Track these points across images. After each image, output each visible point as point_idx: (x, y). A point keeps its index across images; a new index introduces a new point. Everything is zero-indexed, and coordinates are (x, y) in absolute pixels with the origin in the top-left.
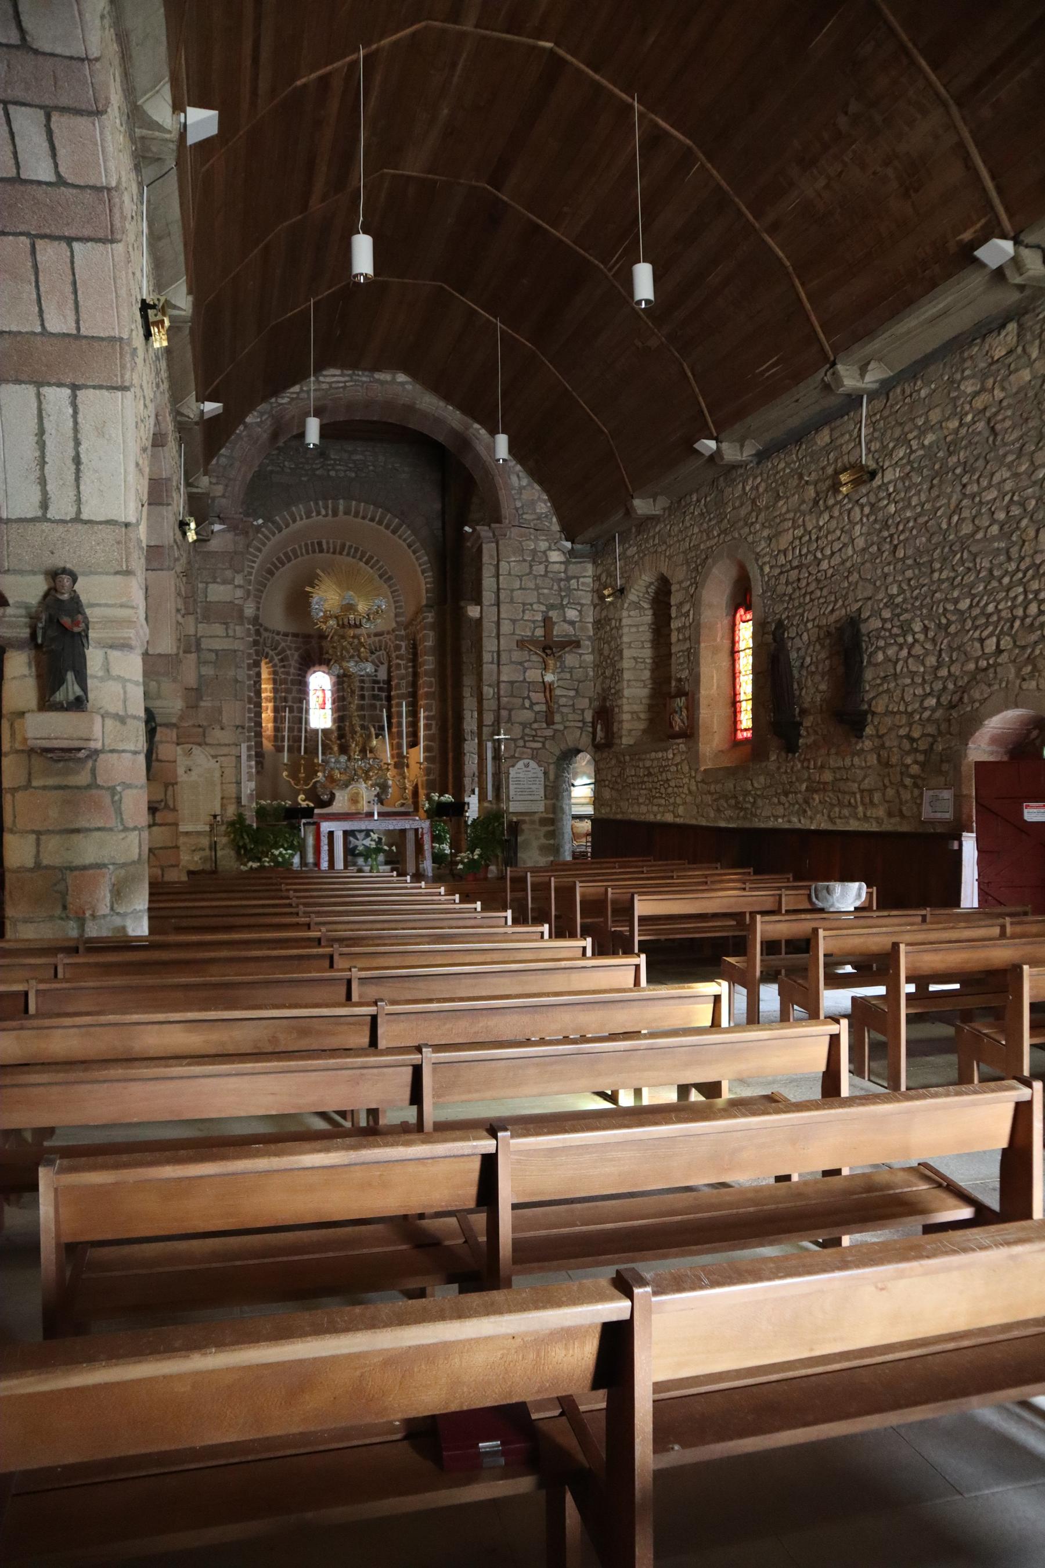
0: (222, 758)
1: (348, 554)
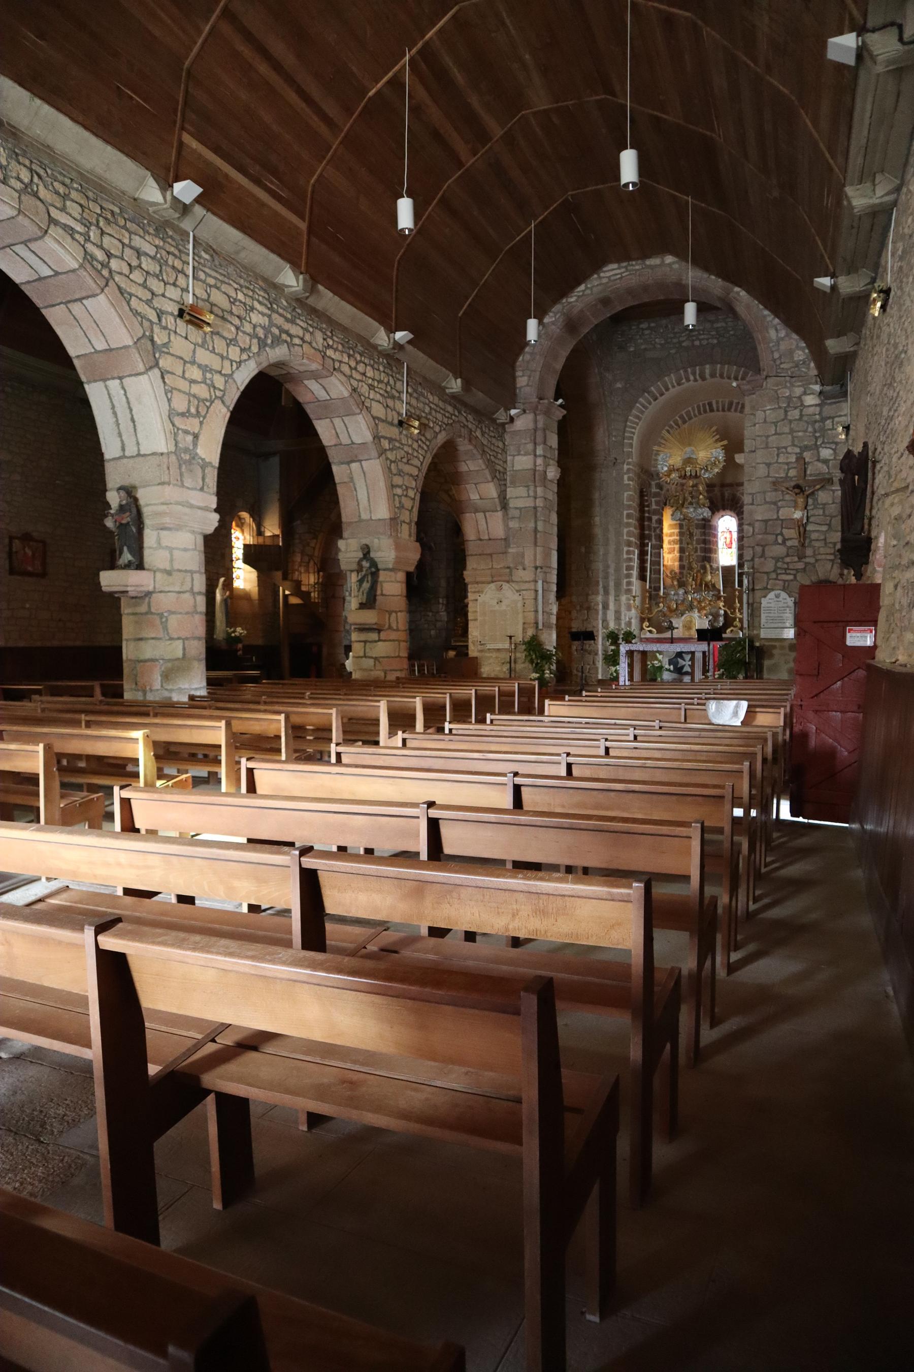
0: (524, 592)
1: (736, 410)
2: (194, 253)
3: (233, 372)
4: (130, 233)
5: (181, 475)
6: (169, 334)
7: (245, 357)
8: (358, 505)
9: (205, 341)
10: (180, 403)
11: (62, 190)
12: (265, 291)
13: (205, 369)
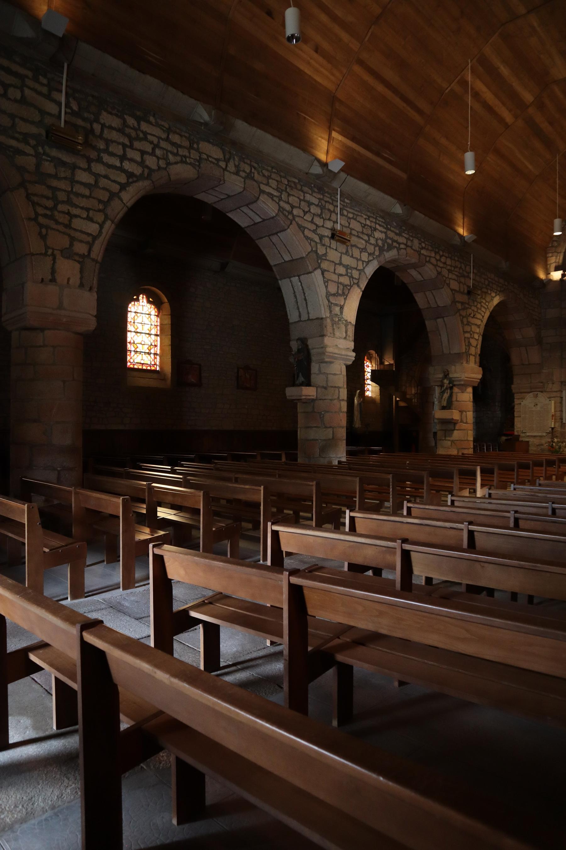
2: (340, 200)
3: (364, 268)
4: (304, 193)
5: (334, 329)
6: (326, 249)
7: (371, 258)
8: (442, 345)
9: (347, 251)
10: (333, 289)
11: (266, 174)
12: (383, 218)
13: (347, 267)
